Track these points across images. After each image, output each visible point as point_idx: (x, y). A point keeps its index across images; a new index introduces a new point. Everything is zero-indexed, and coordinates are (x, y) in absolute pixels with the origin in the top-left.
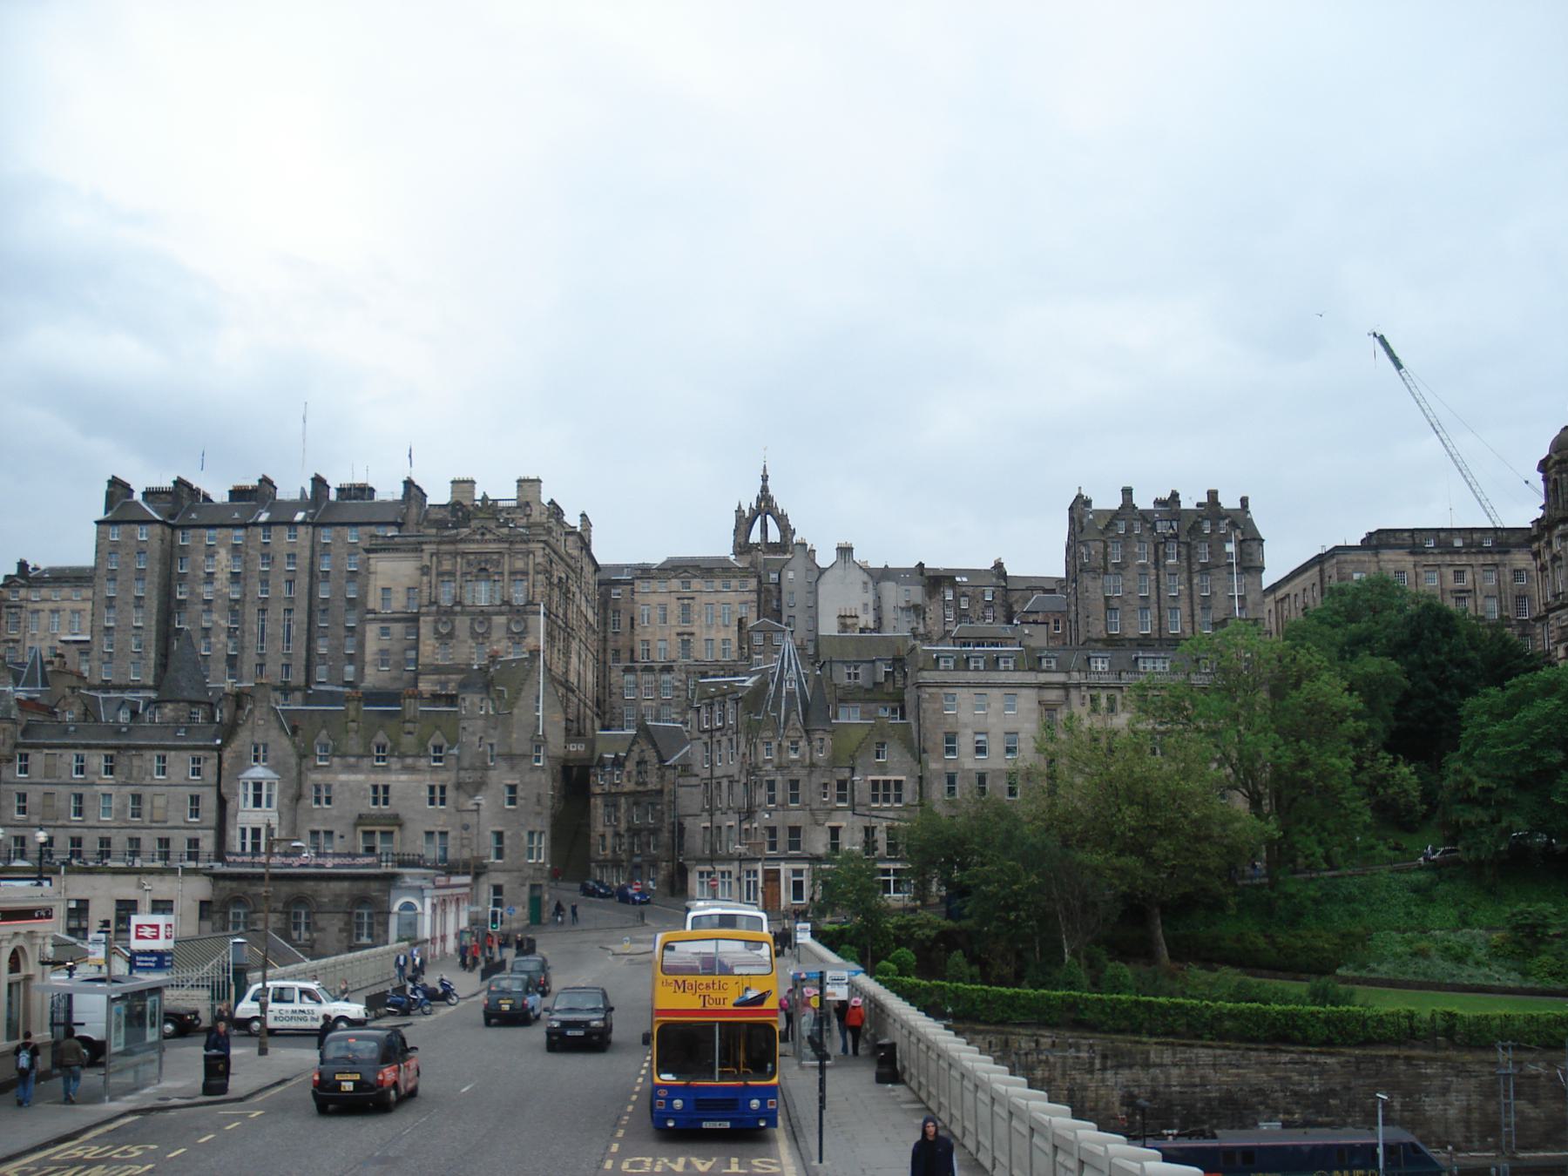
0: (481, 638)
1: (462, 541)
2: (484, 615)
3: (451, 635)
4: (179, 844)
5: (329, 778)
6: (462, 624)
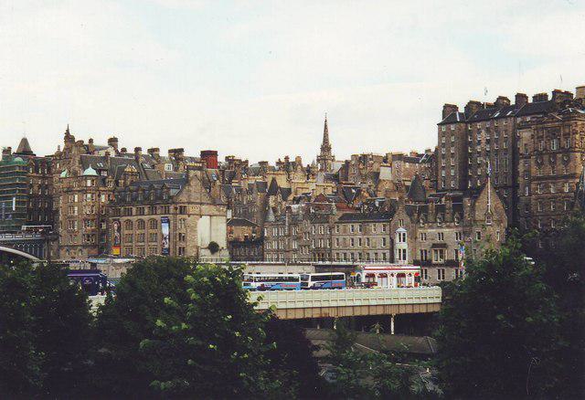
0: (553, 164)
1: (545, 123)
2: (554, 154)
3: (542, 164)
4: (380, 252)
5: (425, 231)
6: (546, 158)
